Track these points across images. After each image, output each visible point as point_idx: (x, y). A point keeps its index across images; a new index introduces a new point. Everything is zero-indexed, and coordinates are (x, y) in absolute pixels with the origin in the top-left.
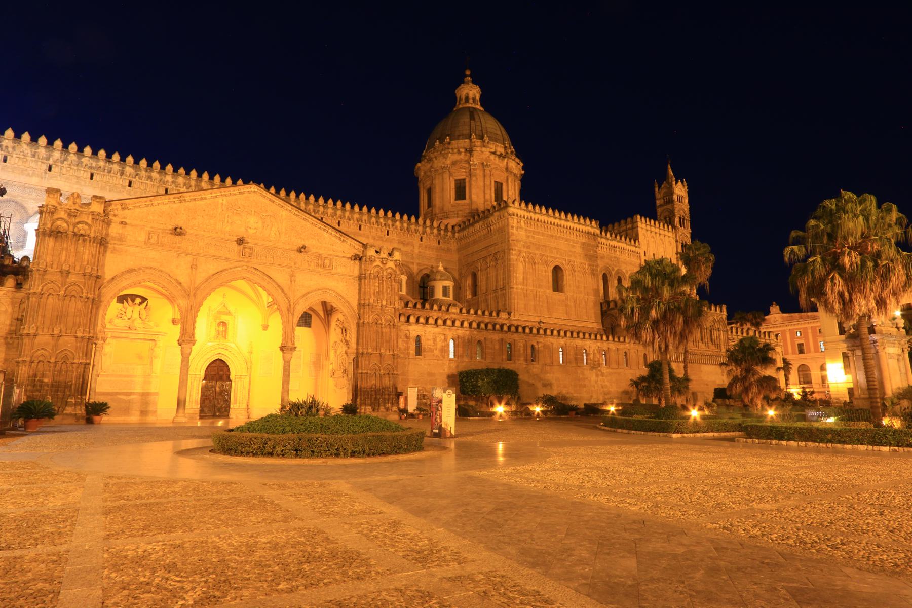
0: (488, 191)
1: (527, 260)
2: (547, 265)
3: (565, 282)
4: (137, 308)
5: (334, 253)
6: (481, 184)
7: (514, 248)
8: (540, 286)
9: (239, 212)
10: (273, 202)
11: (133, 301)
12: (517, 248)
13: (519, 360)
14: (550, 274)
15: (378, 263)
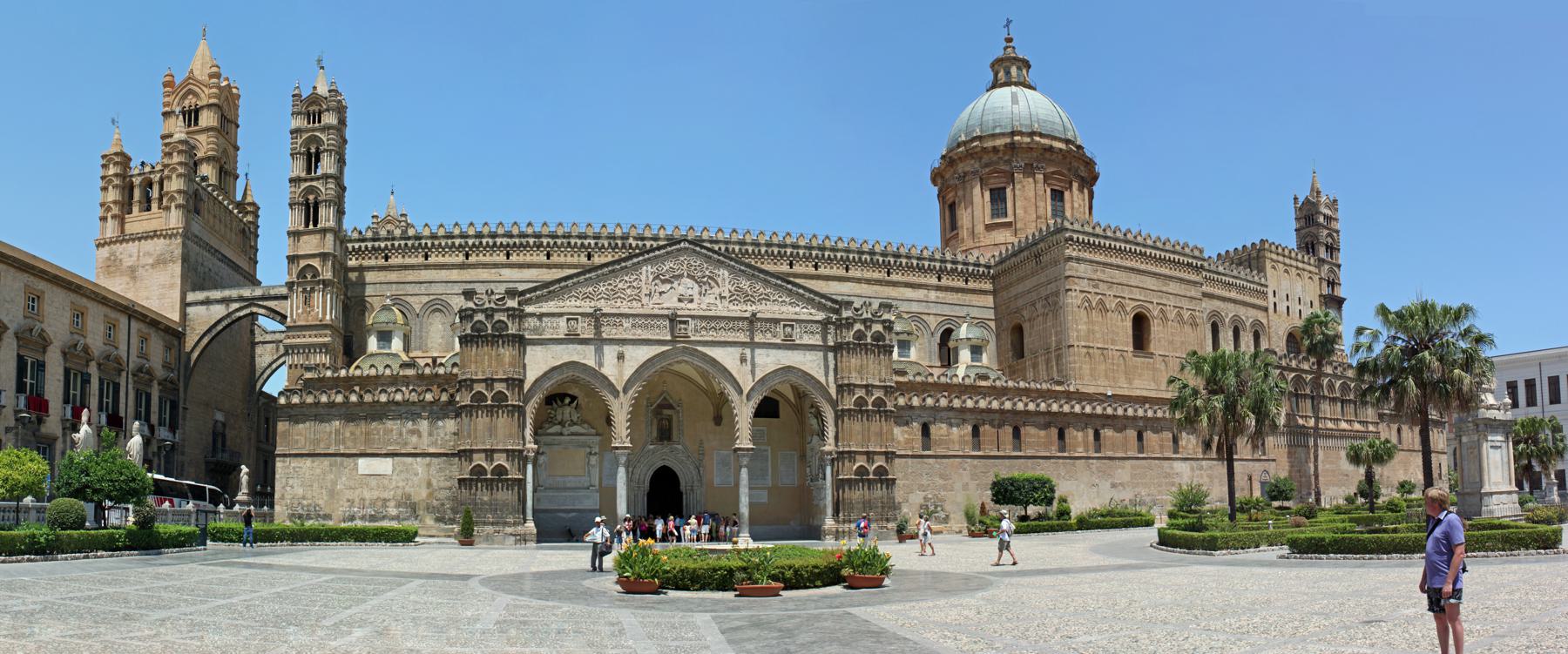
0: (1041, 204)
1: (1094, 304)
2: (1126, 313)
3: (1152, 336)
4: (567, 410)
5: (796, 317)
6: (1032, 194)
7: (1073, 288)
8: (1113, 342)
9: (667, 277)
10: (710, 257)
11: (562, 401)
12: (1078, 288)
13: (1075, 451)
14: (1129, 324)
15: (858, 326)
